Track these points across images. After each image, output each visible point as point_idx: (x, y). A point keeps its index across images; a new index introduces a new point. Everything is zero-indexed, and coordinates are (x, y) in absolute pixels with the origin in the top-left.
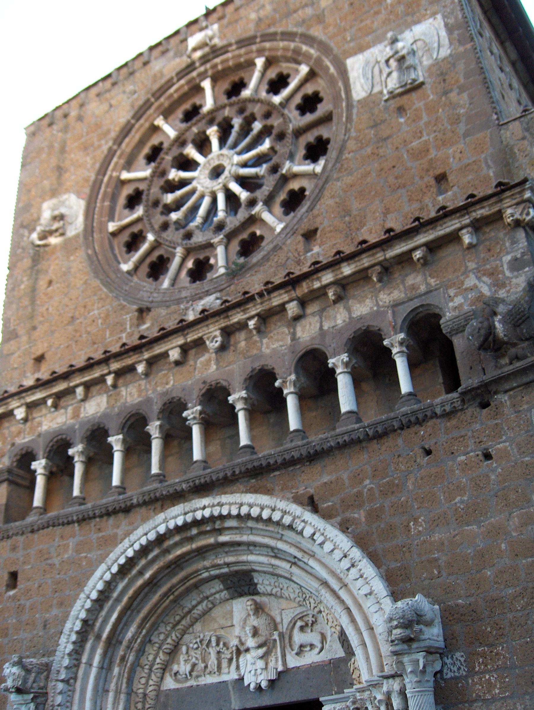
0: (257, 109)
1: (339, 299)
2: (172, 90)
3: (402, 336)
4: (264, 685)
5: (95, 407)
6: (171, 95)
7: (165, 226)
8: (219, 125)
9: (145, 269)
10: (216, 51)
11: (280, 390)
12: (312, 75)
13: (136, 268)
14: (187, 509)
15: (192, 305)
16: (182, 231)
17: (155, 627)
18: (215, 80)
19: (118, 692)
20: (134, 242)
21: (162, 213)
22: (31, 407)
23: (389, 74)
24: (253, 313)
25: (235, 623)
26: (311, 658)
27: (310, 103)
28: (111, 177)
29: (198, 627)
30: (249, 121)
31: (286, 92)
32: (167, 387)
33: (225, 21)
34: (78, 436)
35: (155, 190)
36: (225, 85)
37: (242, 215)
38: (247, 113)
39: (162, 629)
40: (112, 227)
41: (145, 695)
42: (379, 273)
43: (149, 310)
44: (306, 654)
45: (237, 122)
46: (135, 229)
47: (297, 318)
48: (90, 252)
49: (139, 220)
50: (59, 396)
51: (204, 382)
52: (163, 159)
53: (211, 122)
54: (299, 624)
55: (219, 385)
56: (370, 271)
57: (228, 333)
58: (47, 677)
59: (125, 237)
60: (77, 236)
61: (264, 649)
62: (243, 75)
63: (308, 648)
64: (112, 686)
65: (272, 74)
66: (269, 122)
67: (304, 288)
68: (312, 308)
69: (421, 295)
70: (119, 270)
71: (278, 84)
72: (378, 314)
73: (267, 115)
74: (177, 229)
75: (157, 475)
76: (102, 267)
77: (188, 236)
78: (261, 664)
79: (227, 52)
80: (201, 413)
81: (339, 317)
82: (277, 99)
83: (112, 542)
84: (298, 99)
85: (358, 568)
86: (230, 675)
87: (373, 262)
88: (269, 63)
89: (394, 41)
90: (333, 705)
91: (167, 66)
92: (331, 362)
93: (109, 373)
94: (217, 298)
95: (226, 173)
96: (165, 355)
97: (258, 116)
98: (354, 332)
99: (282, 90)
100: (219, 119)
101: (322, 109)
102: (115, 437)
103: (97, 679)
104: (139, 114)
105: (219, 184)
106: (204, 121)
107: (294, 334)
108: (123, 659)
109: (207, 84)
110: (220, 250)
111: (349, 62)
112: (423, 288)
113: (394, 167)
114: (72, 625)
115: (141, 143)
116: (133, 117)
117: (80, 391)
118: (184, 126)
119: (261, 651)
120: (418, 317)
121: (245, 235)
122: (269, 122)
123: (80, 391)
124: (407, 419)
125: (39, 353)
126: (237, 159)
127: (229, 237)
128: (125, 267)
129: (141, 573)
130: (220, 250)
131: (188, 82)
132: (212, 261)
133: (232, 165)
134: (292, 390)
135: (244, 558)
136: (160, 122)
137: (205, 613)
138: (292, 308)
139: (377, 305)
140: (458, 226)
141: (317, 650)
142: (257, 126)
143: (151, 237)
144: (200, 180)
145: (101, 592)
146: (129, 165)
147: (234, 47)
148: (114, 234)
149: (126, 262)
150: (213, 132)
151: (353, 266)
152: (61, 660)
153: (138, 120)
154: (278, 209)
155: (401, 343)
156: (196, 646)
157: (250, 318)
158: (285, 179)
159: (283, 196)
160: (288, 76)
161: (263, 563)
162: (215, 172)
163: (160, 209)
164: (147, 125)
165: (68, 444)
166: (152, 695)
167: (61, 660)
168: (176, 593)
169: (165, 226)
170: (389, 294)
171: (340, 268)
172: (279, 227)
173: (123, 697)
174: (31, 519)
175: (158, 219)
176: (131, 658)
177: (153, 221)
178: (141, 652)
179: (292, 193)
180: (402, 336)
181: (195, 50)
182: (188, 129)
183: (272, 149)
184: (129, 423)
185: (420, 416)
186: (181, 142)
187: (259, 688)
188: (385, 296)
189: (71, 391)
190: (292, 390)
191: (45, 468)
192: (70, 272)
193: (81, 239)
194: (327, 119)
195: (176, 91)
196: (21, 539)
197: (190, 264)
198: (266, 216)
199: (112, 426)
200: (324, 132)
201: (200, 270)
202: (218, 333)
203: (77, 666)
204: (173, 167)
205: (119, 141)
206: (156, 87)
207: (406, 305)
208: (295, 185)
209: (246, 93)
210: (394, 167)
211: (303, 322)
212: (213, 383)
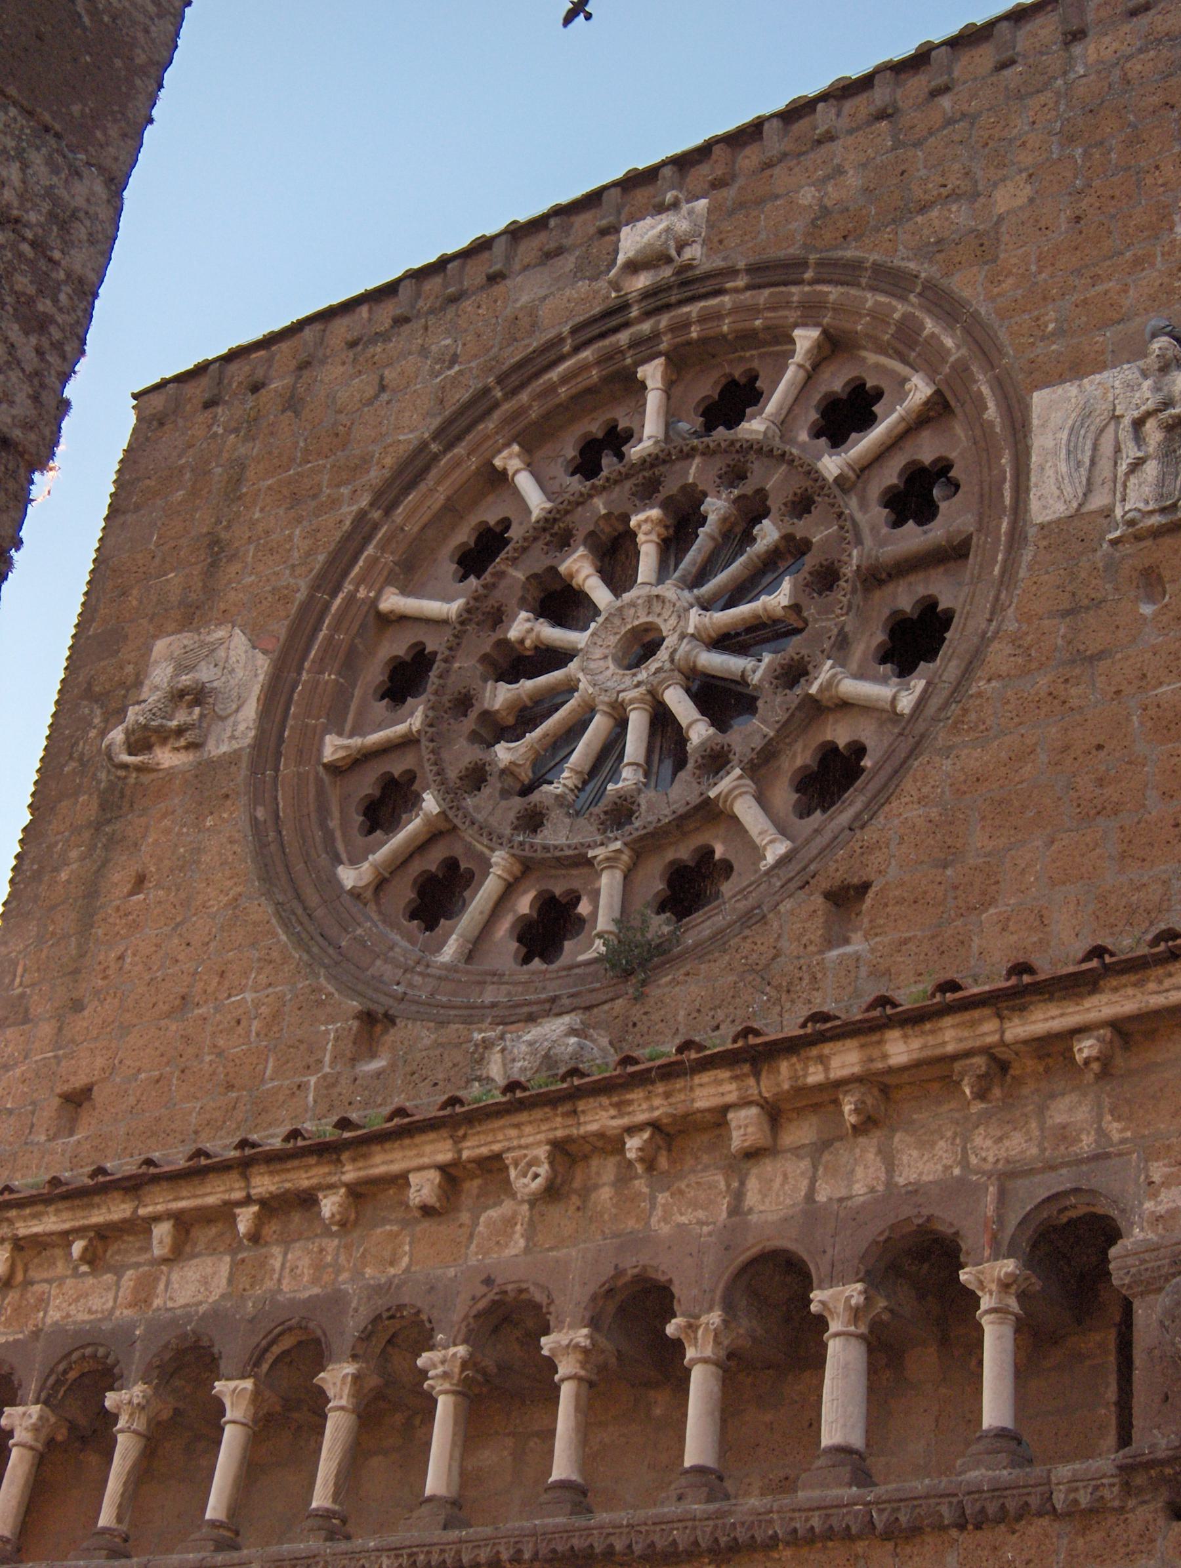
0: (776, 482)
1: (867, 1123)
2: (554, 375)
3: (1008, 1266)
5: (197, 1286)
6: (552, 389)
7: (476, 777)
8: (665, 505)
9: (404, 893)
10: (691, 284)
11: (677, 1346)
12: (937, 410)
13: (381, 884)
15: (502, 1037)
16: (517, 802)
18: (679, 365)
20: (387, 805)
21: (474, 737)
23: (1137, 465)
24: (641, 1117)
27: (914, 497)
28: (351, 598)
30: (753, 510)
31: (865, 443)
32: (392, 1271)
33: (729, 194)
34: (137, 1361)
35: (467, 665)
36: (706, 387)
37: (682, 792)
38: (747, 488)
40: (333, 747)
42: (980, 1077)
43: (390, 1020)
45: (716, 507)
46: (397, 767)
47: (752, 1155)
48: (260, 813)
49: (408, 742)
50: (103, 1235)
51: (488, 1281)
52: (501, 575)
53: (648, 491)
55: (524, 1296)
56: (958, 1066)
57: (567, 1153)
59: (366, 784)
60: (233, 759)
62: (756, 364)
65: (836, 381)
66: (801, 528)
67: (784, 1075)
69: (1079, 1162)
70: (335, 881)
71: (846, 414)
72: (958, 1189)
73: (802, 506)
74: (505, 794)
75: (326, 1515)
76: (285, 870)
77: (533, 820)
79: (719, 292)
80: (464, 1365)
81: (859, 1176)
82: (831, 465)
84: (890, 475)
87: (968, 1045)
88: (834, 346)
91: (551, 300)
92: (817, 1295)
93: (248, 1201)
94: (573, 1032)
95: (663, 654)
96: (400, 1181)
97: (775, 503)
98: (892, 1228)
99: (854, 435)
100: (670, 487)
101: (953, 517)
102: (232, 1384)
104: (454, 430)
105: (638, 685)
107: (739, 1196)
109: (652, 373)
110: (609, 883)
111: (1039, 399)
112: (1087, 1143)
113: (1100, 747)
115: (452, 511)
116: (437, 435)
117: (162, 1231)
118: (575, 484)
120: (1064, 1219)
121: (683, 852)
122: (801, 528)
123: (162, 1231)
124: (978, 1506)
125: (79, 1081)
126: (695, 619)
127: (641, 849)
128: (349, 877)
130: (609, 883)
131: (604, 359)
132: (584, 908)
133: (683, 636)
134: (708, 1352)
136: (510, 460)
138: (745, 1127)
139: (964, 1163)
142: (768, 533)
143: (430, 803)
144: (592, 665)
146: (408, 573)
147: (740, 282)
148: (334, 769)
149: (354, 861)
150: (647, 521)
151: (916, 1044)
153: (450, 446)
154: (784, 796)
155: (1005, 1286)
157: (631, 1130)
158: (816, 709)
159: (800, 756)
160: (878, 395)
162: (638, 637)
163: (469, 723)
164: (473, 463)
165: (106, 1376)
169: (476, 777)
170: (1000, 1139)
171: (880, 1042)
172: (776, 850)
175: (462, 754)
177: (445, 755)
179: (829, 752)
180: (1008, 1266)
181: (633, 267)
182: (583, 500)
183: (795, 608)
184: (276, 1350)
185: (1012, 1505)
186: (556, 533)
188: (989, 1143)
189: (139, 1227)
190: (708, 1352)
192: (198, 862)
193: (242, 773)
194: (954, 553)
195: (565, 379)
197: (524, 904)
198: (747, 811)
199: (232, 1349)
200: (945, 590)
201: (551, 927)
202: (542, 1152)
204: (523, 604)
205: (389, 496)
206: (515, 355)
207: (1037, 1179)
208: (840, 733)
209: (755, 426)
210: (1100, 747)
211: (768, 1167)
212: (509, 1287)
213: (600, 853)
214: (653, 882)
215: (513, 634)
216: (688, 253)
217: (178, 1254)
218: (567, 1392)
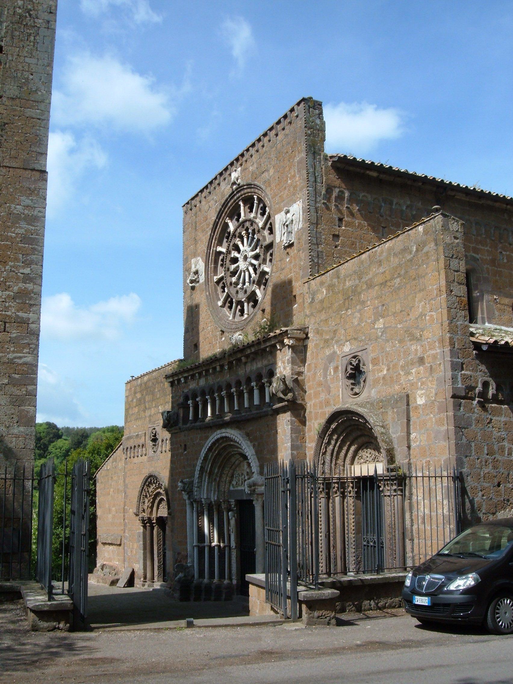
5: (202, 382)
17: (223, 470)
19: (215, 491)
22: (186, 378)
29: (237, 469)
39: (226, 469)
40: (215, 278)
41: (224, 491)
48: (207, 294)
58: (193, 486)
64: (213, 489)
68: (249, 360)
70: (217, 305)
72: (262, 368)
75: (218, 415)
80: (226, 393)
83: (207, 438)
89: (288, 212)
103: (208, 486)
106: (241, 226)
108: (215, 479)
109: (241, 203)
110: (246, 304)
114: (198, 468)
116: (217, 218)
117: (197, 375)
123: (197, 375)
129: (215, 451)
137: (239, 464)
140: (275, 342)
145: (204, 457)
150: (244, 233)
152: (196, 481)
155: (267, 382)
163: (229, 274)
166: (227, 491)
167: (196, 481)
173: (216, 493)
174: (188, 425)
176: (218, 479)
178: (221, 477)
191: (192, 404)
196: (186, 432)
199: (207, 391)
203: (202, 482)
204: (233, 250)
213: (243, 300)
214: (251, 304)
215: (232, 256)
216: (239, 181)
217: (200, 378)
218: (235, 397)
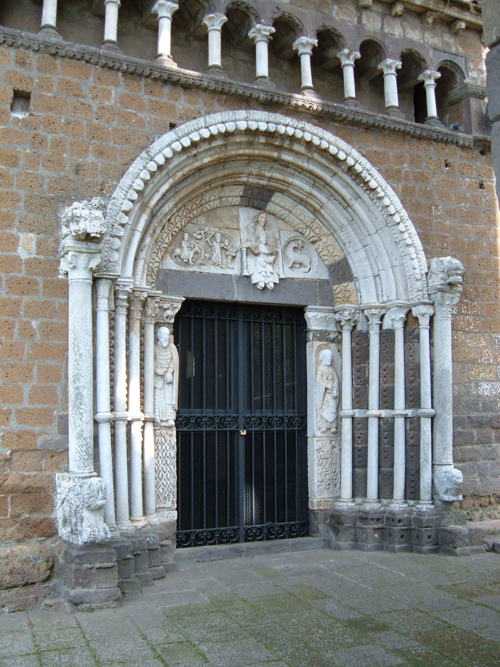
4: (271, 286)
14: (271, 119)
25: (241, 227)
26: (298, 274)
44: (295, 269)
54: (293, 245)
55: (290, 19)
61: (273, 257)
63: (298, 266)
78: (269, 268)
85: (406, 224)
86: (233, 270)
90: (316, 313)
119: (271, 258)
135: (290, 180)
141: (307, 269)
156: (200, 237)
161: (303, 190)
168: (213, 185)
187: (265, 288)
212: (286, 14)
